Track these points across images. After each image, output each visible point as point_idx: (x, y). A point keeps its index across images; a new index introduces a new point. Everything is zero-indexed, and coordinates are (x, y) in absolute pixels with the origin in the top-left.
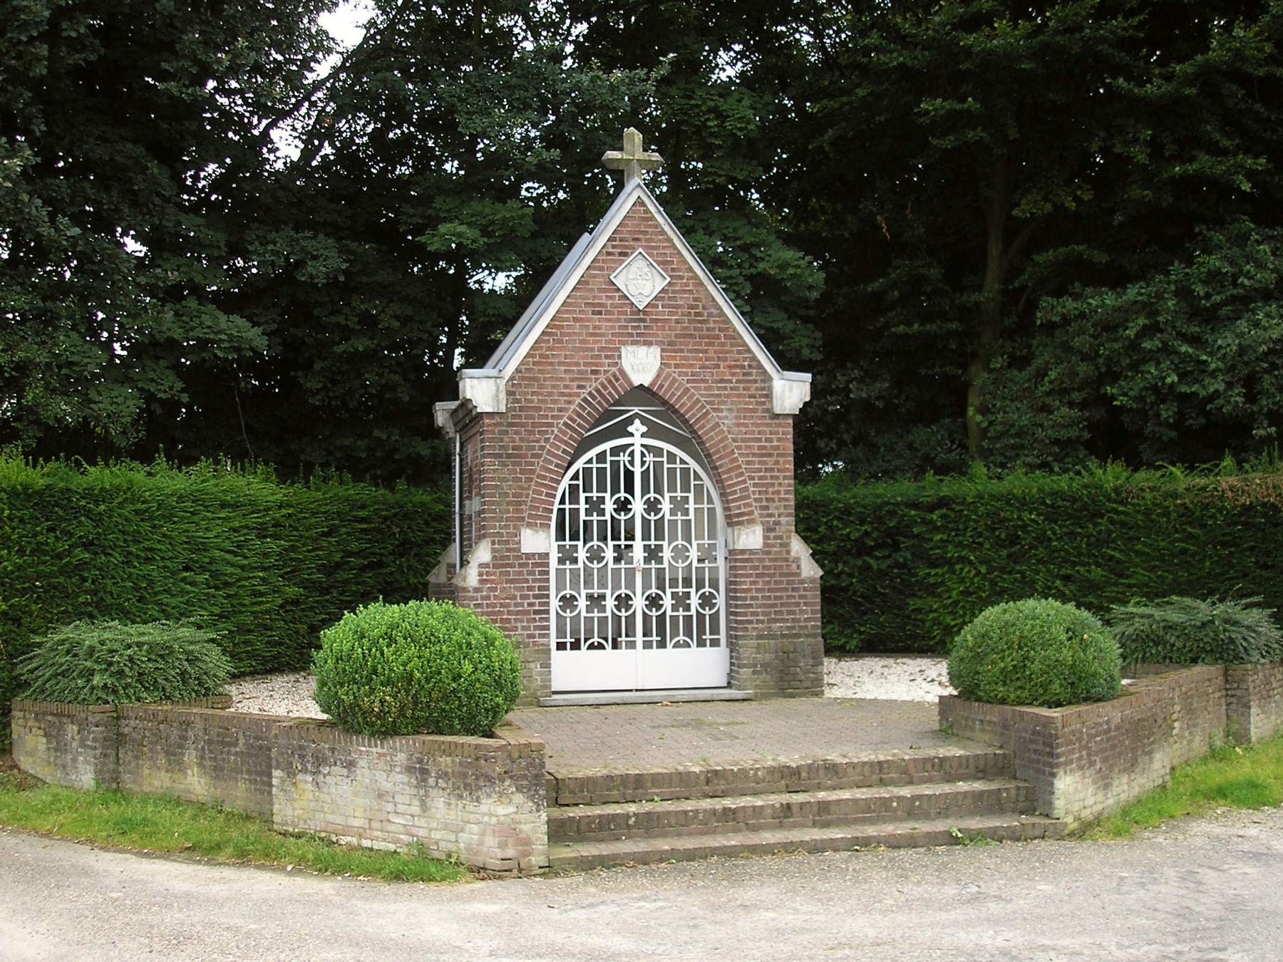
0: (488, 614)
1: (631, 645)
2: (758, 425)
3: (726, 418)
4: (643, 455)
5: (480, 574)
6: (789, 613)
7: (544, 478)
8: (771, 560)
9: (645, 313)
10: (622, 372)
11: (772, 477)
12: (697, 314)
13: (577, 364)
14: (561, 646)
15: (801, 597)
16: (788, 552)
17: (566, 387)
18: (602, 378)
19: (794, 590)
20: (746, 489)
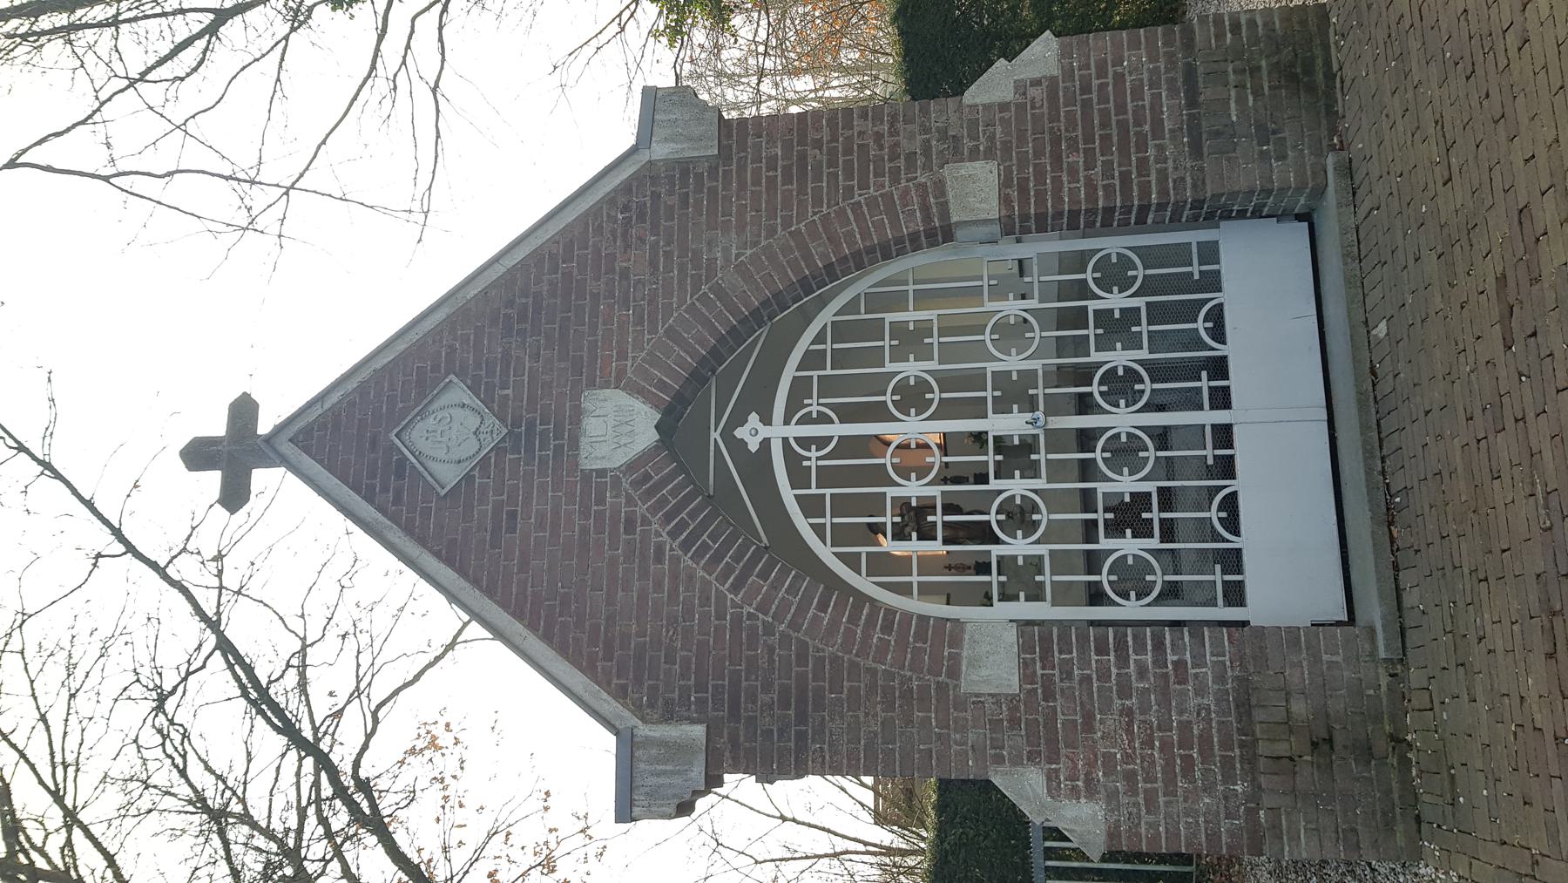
0: (1170, 781)
1: (1224, 435)
2: (742, 186)
3: (726, 250)
4: (806, 420)
5: (1075, 793)
6: (1137, 93)
7: (849, 634)
8: (1022, 139)
9: (516, 423)
10: (631, 466)
11: (848, 151)
12: (522, 317)
13: (613, 562)
14: (1235, 594)
15: (1102, 73)
16: (1004, 107)
17: (658, 586)
18: (641, 509)
19: (1086, 89)
20: (872, 203)
